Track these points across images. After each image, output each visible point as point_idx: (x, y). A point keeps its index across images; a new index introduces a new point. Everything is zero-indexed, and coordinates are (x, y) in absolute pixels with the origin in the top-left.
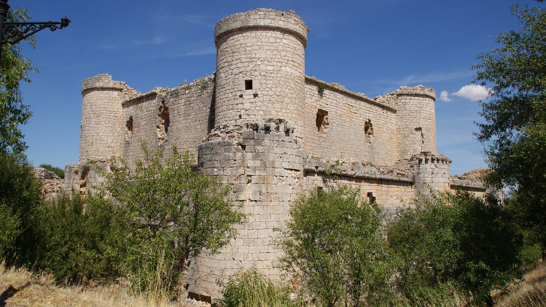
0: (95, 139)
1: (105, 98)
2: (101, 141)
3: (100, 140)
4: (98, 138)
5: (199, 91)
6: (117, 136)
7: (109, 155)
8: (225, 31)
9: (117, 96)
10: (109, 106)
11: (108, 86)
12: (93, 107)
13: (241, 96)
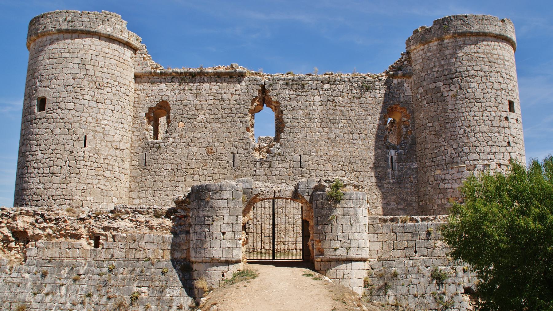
0: (93, 131)
1: (112, 56)
2: (104, 135)
3: (103, 133)
4: (97, 128)
5: (354, 91)
6: (127, 131)
7: (117, 164)
8: (477, 31)
9: (130, 60)
10: (119, 74)
11: (120, 37)
13: (507, 118)
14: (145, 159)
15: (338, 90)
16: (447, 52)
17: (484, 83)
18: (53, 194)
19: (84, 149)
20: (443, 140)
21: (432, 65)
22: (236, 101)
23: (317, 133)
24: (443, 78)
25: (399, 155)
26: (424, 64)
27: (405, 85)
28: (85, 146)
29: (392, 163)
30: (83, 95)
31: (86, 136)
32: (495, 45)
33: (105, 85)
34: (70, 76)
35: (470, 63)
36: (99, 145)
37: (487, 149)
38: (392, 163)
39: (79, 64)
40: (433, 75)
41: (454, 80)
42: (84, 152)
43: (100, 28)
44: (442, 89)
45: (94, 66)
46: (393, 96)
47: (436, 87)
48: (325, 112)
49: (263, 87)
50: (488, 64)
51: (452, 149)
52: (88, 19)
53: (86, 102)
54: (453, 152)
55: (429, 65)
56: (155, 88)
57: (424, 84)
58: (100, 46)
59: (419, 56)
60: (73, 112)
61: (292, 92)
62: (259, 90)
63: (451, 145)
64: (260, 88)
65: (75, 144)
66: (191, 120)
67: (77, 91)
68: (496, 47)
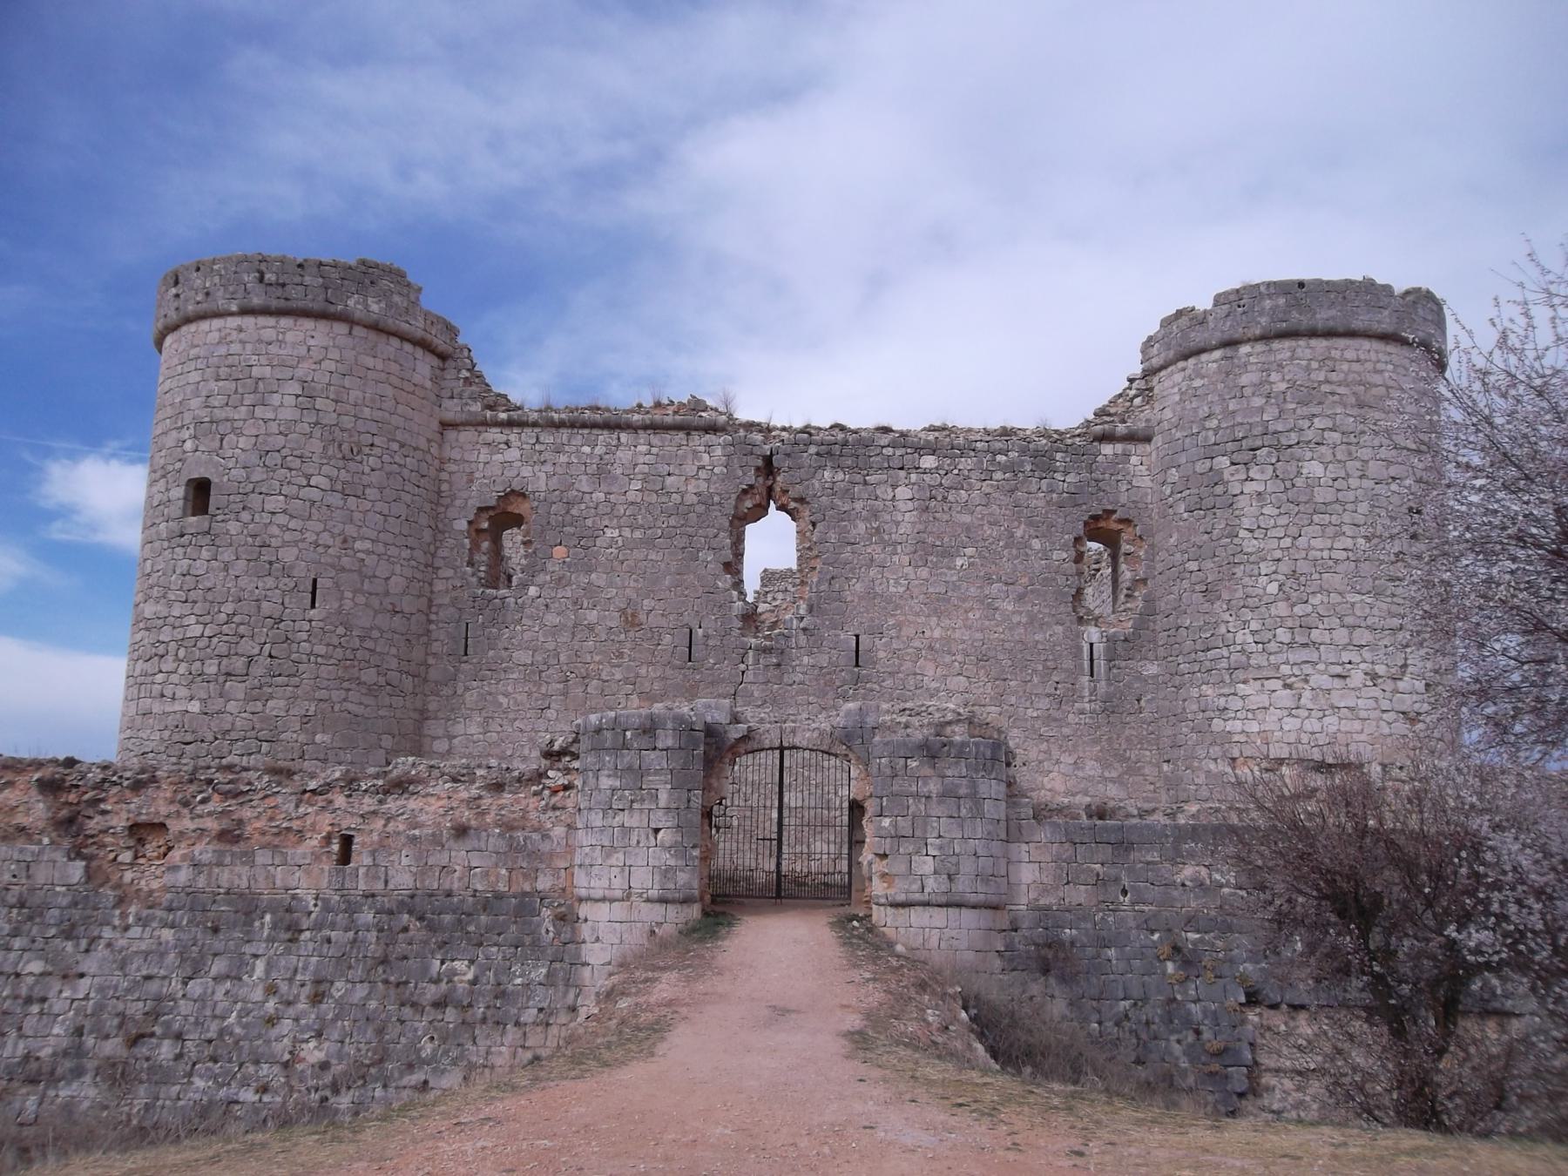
0: (333, 566)
2: (363, 577)
3: (359, 572)
4: (345, 561)
6: (422, 567)
7: (394, 651)
12: (319, 403)
14: (467, 639)
15: (956, 472)
16: (1244, 380)
17: (1339, 462)
18: (228, 726)
19: (312, 612)
20: (1225, 607)
21: (1204, 410)
22: (697, 494)
23: (902, 581)
24: (1230, 446)
25: (1111, 640)
26: (1184, 409)
27: (1134, 460)
28: (313, 606)
29: (1092, 660)
30: (308, 477)
31: (315, 581)
32: (1378, 361)
33: (366, 450)
34: (274, 427)
35: (1305, 411)
36: (348, 604)
37: (1341, 635)
38: (1092, 660)
39: (297, 396)
40: (1206, 438)
41: (1258, 452)
42: (310, 621)
43: (351, 303)
44: (1226, 476)
45: (337, 402)
46: (1100, 489)
47: (1211, 469)
48: (921, 527)
49: (768, 460)
50: (1355, 411)
51: (1247, 631)
52: (321, 280)
53: (315, 494)
54: (1250, 639)
55: (1195, 410)
56: (494, 457)
57: (1183, 459)
58: (353, 349)
59: (1173, 387)
60: (282, 519)
61: (840, 476)
62: (758, 469)
63: (1245, 622)
64: (760, 463)
65: (287, 600)
66: (586, 539)
67: (292, 465)
68: (1380, 366)
